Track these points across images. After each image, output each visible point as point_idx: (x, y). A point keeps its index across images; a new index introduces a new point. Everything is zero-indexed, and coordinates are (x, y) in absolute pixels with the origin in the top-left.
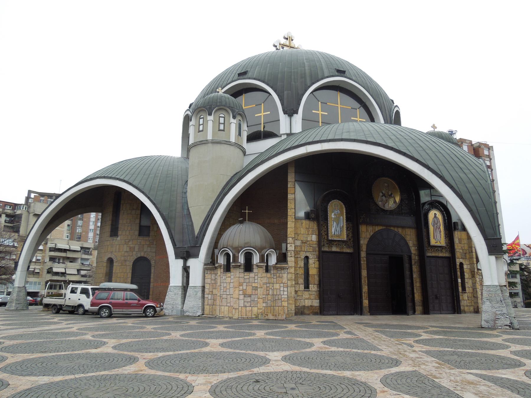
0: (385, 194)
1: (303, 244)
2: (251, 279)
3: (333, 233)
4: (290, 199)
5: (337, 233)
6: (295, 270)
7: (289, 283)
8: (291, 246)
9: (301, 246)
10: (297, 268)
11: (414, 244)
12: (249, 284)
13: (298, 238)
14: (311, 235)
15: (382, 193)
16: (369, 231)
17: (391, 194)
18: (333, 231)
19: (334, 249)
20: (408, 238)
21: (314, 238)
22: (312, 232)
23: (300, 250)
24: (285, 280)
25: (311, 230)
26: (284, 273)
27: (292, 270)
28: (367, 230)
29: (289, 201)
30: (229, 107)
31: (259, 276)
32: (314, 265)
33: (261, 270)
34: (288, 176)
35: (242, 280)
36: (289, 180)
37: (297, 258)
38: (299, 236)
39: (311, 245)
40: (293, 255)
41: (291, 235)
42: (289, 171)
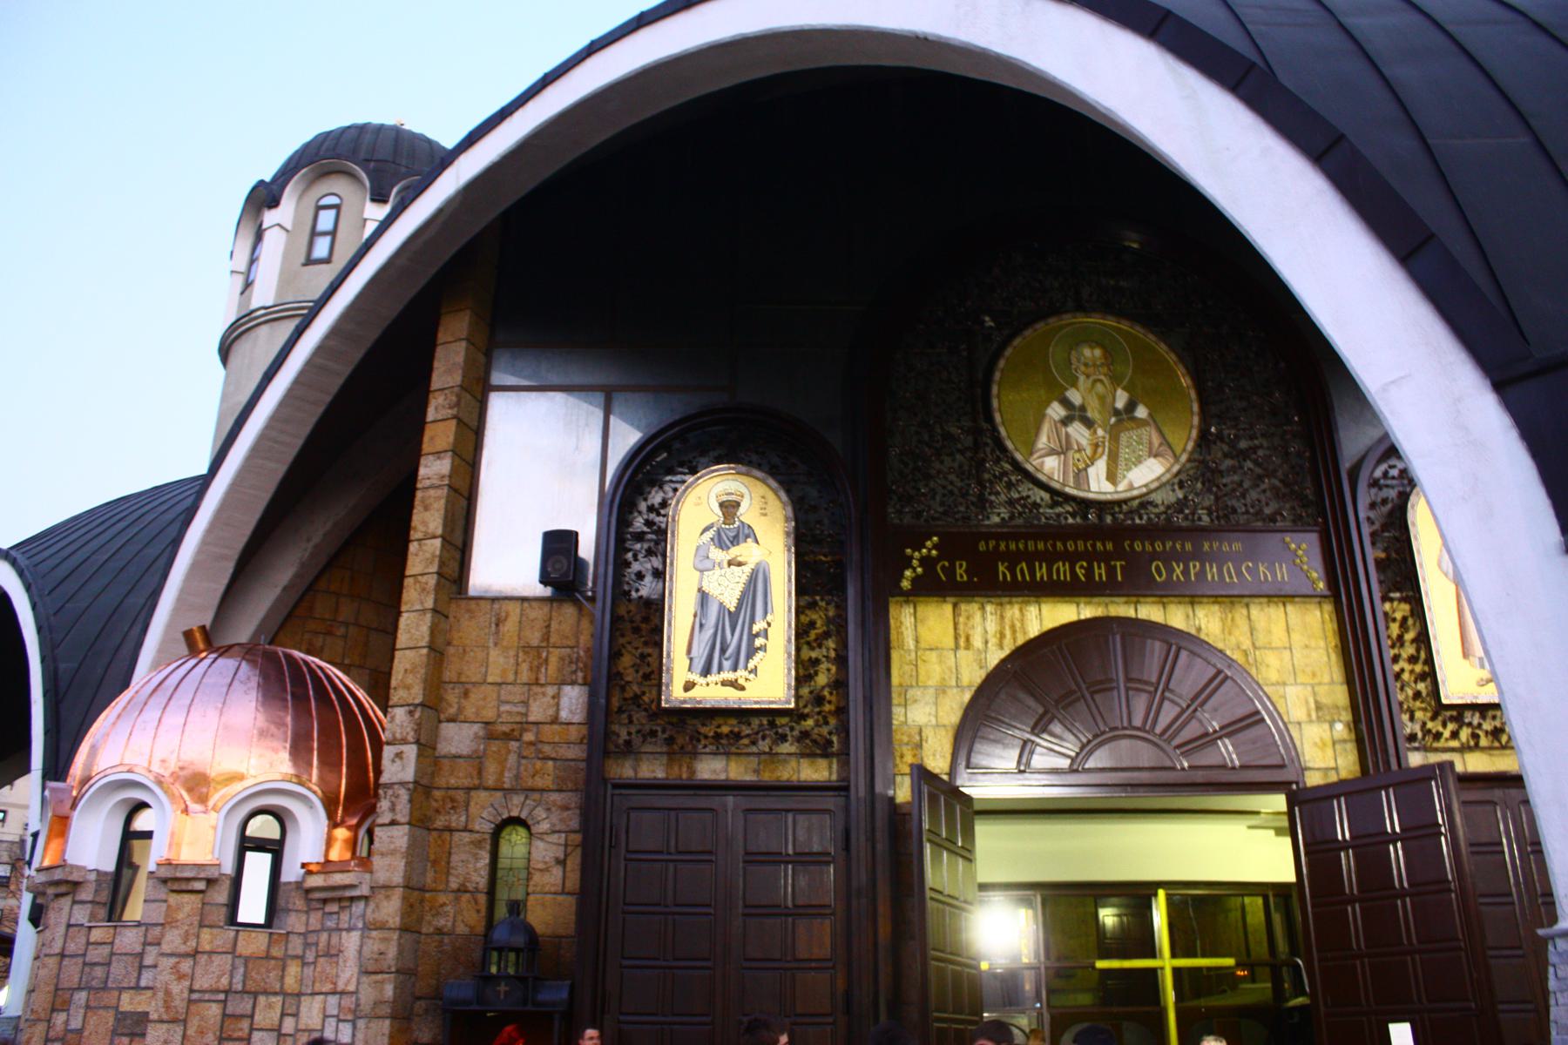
0: (1083, 408)
1: (495, 746)
2: (117, 969)
3: (699, 664)
4: (427, 483)
5: (727, 664)
6: (409, 908)
7: (367, 995)
8: (399, 755)
9: (477, 760)
10: (442, 898)
11: (1319, 707)
12: (105, 995)
13: (461, 709)
14: (551, 691)
15: (1066, 403)
16: (977, 642)
17: (1131, 406)
18: (700, 652)
19: (710, 768)
20: (1271, 669)
21: (573, 701)
22: (560, 670)
23: (466, 782)
24: (348, 974)
25: (553, 660)
26: (349, 930)
27: (390, 909)
28: (961, 640)
29: (419, 494)
30: (362, 165)
31: (166, 948)
32: (557, 872)
33: (189, 903)
34: (436, 364)
35: (72, 972)
36: (437, 381)
37: (451, 830)
38: (473, 696)
39: (547, 749)
40: (403, 813)
41: (408, 688)
42: (441, 337)
